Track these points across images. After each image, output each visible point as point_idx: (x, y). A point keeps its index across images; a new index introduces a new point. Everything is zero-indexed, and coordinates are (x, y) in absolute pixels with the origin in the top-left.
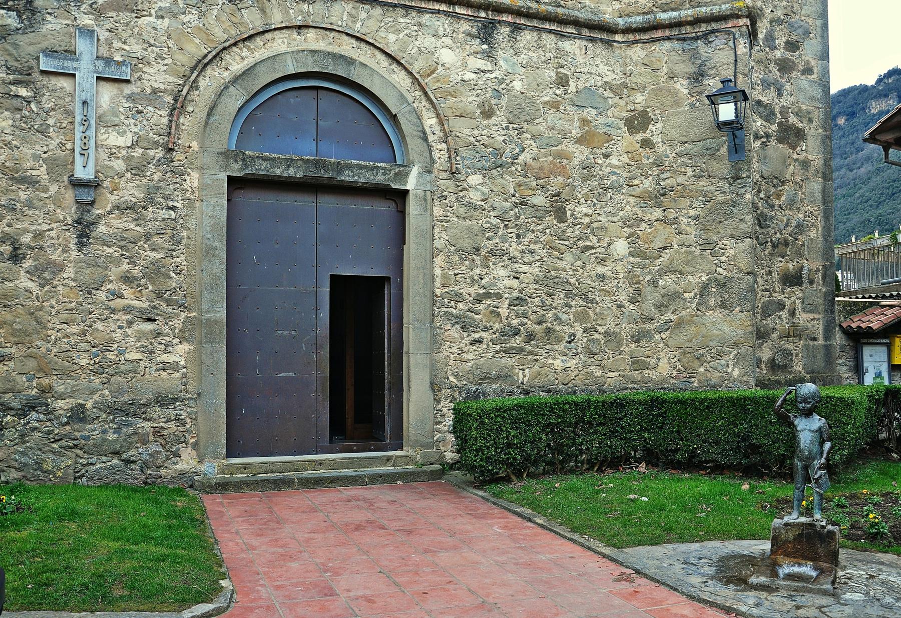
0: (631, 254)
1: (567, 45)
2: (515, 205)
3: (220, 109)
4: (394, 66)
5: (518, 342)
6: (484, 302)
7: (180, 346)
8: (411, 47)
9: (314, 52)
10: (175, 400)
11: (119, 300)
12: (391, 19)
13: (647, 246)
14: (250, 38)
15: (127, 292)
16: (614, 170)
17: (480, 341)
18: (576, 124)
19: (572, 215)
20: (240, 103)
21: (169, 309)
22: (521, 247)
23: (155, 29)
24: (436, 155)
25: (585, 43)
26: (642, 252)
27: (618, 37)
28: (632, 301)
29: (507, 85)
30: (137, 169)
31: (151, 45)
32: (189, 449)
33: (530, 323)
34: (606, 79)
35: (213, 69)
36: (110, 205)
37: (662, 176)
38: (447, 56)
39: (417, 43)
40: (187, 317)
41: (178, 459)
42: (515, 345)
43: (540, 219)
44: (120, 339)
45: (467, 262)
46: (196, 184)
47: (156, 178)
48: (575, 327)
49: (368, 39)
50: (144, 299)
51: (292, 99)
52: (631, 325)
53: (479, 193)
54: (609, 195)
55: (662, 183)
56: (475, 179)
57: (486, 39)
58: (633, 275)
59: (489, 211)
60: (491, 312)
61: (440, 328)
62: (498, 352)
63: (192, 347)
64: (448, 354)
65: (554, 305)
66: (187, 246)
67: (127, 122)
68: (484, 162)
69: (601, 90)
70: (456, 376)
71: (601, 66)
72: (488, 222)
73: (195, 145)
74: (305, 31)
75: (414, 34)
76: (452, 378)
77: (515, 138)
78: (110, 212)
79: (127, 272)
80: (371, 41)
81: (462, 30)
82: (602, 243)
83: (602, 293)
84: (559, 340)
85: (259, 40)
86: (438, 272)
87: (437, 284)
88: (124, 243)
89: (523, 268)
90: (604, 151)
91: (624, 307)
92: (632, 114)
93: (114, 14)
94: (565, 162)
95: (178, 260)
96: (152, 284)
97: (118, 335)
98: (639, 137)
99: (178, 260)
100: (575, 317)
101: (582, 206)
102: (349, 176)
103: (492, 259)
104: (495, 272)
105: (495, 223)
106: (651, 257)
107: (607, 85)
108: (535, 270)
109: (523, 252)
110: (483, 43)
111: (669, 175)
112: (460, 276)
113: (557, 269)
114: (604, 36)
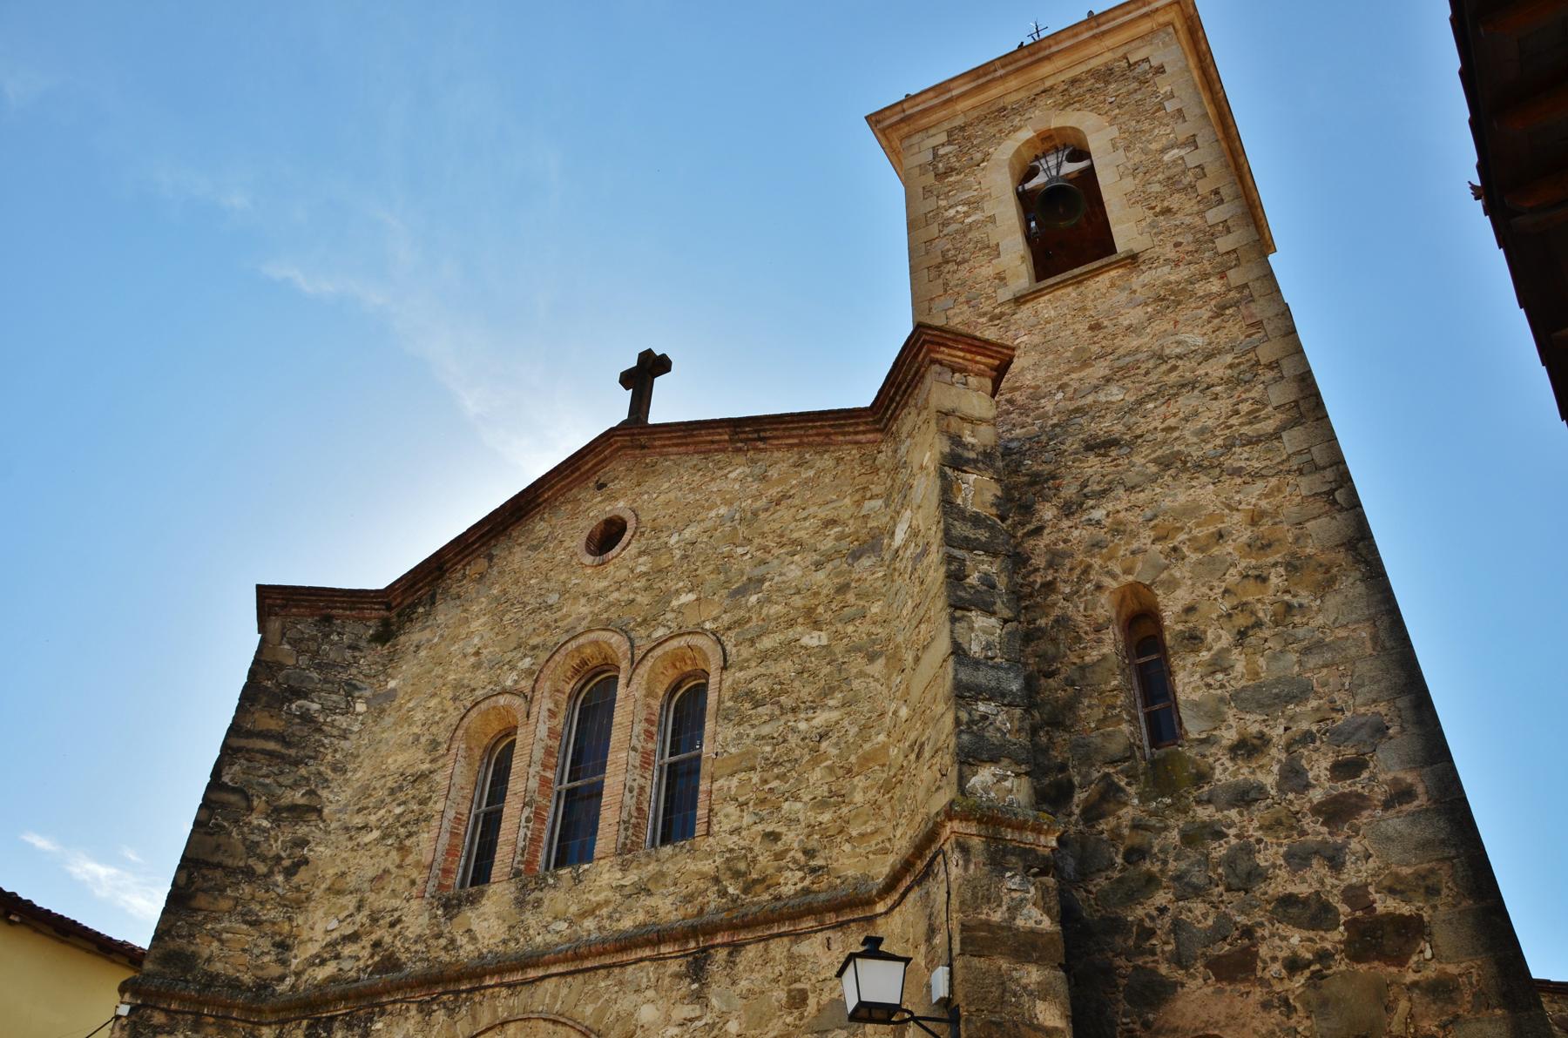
1: (804, 948)
27: (880, 908)
29: (720, 1029)
57: (697, 975)
74: (506, 1027)
75: (614, 996)
110: (694, 982)
114: (859, 914)
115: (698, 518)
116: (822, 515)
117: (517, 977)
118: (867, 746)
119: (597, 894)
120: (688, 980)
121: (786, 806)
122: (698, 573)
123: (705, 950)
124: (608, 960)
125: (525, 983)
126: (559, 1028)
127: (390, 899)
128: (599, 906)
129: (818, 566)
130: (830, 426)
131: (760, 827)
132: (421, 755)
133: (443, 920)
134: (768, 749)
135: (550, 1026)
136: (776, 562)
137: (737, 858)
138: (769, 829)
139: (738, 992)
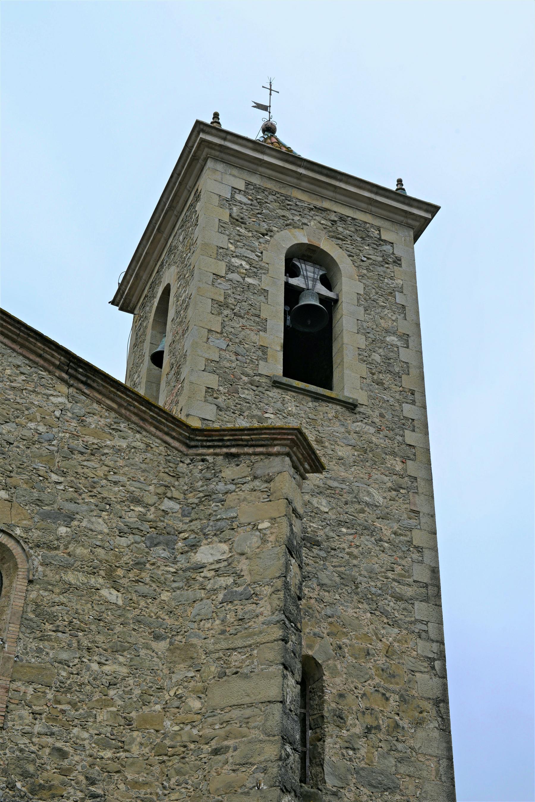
115: (17, 420)
118: (146, 709)
121: (75, 730)
122: (12, 474)
129: (122, 533)
130: (152, 417)
131: (50, 740)
134: (64, 674)
136: (85, 507)
137: (27, 759)
138: (59, 745)
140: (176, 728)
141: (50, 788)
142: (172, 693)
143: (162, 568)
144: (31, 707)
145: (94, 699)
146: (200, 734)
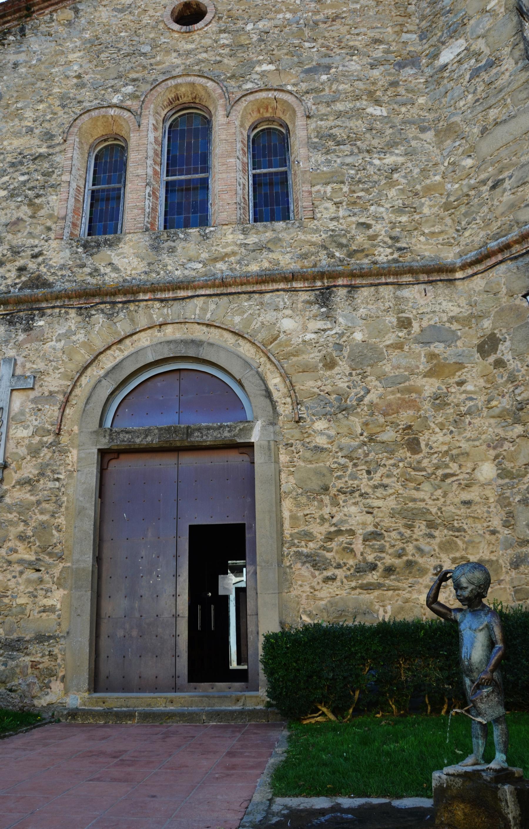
0: (499, 476)
1: (406, 293)
2: (364, 444)
3: (94, 399)
4: (241, 341)
5: (375, 577)
6: (336, 539)
7: (57, 592)
8: (254, 323)
9: (169, 342)
10: (50, 637)
11: (15, 555)
12: (236, 305)
13: (512, 465)
14: (120, 341)
15: (21, 547)
16: (470, 395)
17: (333, 579)
18: (423, 360)
19: (427, 445)
20: (109, 391)
21: (51, 561)
22: (371, 483)
23: (54, 349)
24: (280, 409)
25: (423, 286)
26: (509, 472)
27: (459, 275)
28: (506, 524)
29: (349, 337)
30: (34, 452)
31: (51, 361)
32: (58, 682)
33: (388, 557)
34: (451, 314)
35: (93, 369)
36: (14, 482)
37: (517, 391)
38: (287, 324)
39: (260, 319)
40: (64, 567)
41: (49, 690)
42: (372, 581)
43: (392, 452)
44: (13, 586)
45: (316, 503)
46: (75, 459)
47: (48, 457)
48: (441, 558)
49: (215, 324)
50: (33, 553)
51: (159, 383)
52: (509, 551)
53: (325, 437)
54: (467, 421)
55: (519, 398)
56: (320, 425)
57: (324, 303)
58: (504, 498)
59: (337, 452)
60: (344, 549)
61: (290, 567)
62: (354, 589)
63: (66, 592)
64: (300, 593)
65: (415, 536)
66: (67, 508)
67: (30, 419)
68: (328, 409)
69: (447, 325)
70: (309, 615)
71: (444, 303)
72: (336, 462)
73: (76, 429)
74: (163, 327)
75: (257, 312)
76: (304, 618)
77: (359, 382)
78: (14, 487)
79: (22, 532)
80: (217, 325)
81: (301, 299)
82: (464, 469)
83: (470, 520)
84: (423, 572)
85: (128, 342)
86: (286, 514)
87: (287, 524)
88: (21, 509)
89: (376, 503)
90: (457, 379)
91: (498, 532)
92: (482, 339)
93: (28, 345)
94: (414, 395)
95: (60, 520)
96: (40, 541)
97: (12, 584)
98: (492, 359)
99: (60, 520)
100: (440, 548)
101: (437, 435)
102: (198, 437)
103: (342, 497)
104: (345, 509)
105: (343, 463)
106: (519, 476)
107: (452, 319)
108: (391, 503)
109: (375, 487)
111: (522, 388)
112: (309, 516)
113: (414, 500)
114: (444, 277)
115: (268, 16)
116: (372, 35)
117: (171, 295)
118: (428, 182)
119: (224, 247)
120: (317, 305)
121: (372, 208)
122: (274, 52)
123: (328, 288)
124: (249, 288)
125: (175, 299)
126: (212, 330)
127: (27, 239)
128: (227, 255)
129: (373, 66)
131: (354, 219)
132: (37, 142)
133: (84, 255)
134: (353, 172)
135: (204, 328)
136: (338, 57)
137: (339, 235)
138: (362, 220)
139: (359, 315)
140: (457, 186)
141: (363, 251)
142: (446, 164)
143: (414, 81)
144: (332, 200)
145: (382, 184)
146: (477, 180)
